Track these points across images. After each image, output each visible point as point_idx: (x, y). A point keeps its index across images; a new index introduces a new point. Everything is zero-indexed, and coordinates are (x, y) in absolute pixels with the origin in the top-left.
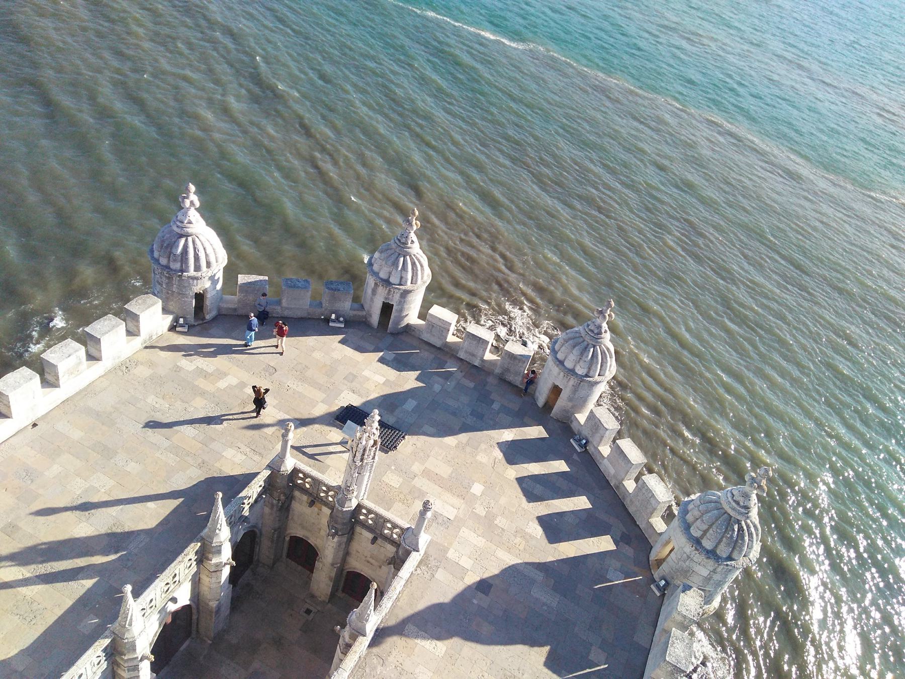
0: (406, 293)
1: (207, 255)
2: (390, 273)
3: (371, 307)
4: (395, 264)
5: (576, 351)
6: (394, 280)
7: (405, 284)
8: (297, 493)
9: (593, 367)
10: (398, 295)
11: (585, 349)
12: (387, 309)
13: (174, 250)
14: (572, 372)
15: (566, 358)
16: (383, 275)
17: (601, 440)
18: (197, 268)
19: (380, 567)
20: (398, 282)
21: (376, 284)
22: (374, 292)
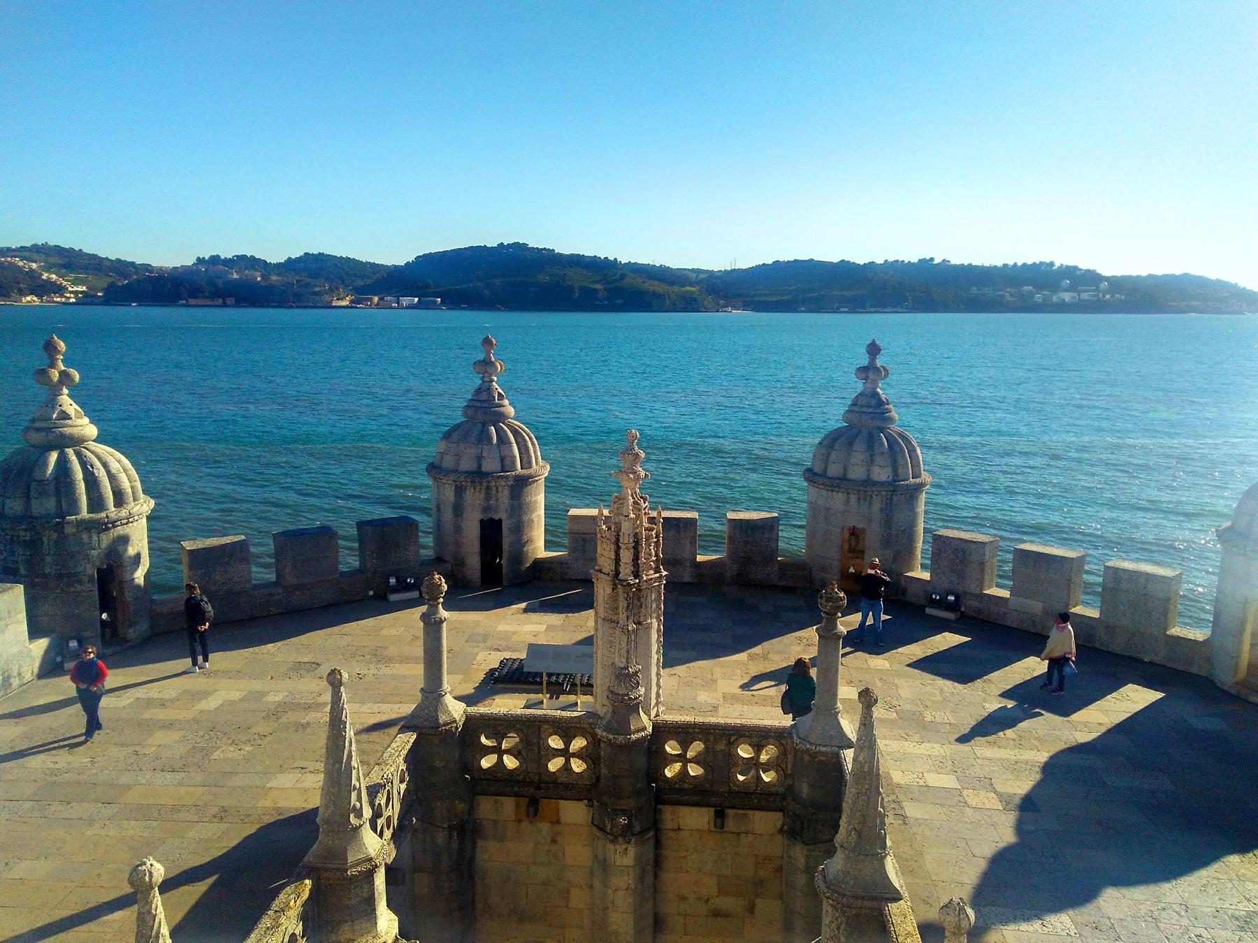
0: (523, 482)
1: (112, 477)
2: (479, 458)
3: (458, 544)
4: (484, 437)
5: (859, 446)
6: (490, 465)
7: (513, 468)
8: (486, 807)
9: (900, 461)
10: (506, 492)
11: (871, 441)
12: (491, 530)
13: (37, 475)
14: (868, 483)
15: (845, 470)
16: (465, 465)
17: (982, 571)
18: (96, 503)
19: (751, 909)
20: (499, 468)
21: (459, 491)
22: (458, 509)
